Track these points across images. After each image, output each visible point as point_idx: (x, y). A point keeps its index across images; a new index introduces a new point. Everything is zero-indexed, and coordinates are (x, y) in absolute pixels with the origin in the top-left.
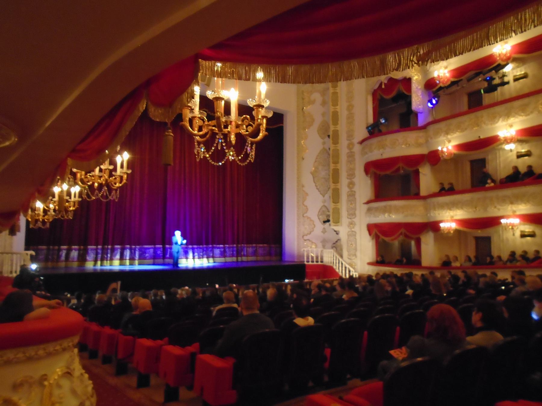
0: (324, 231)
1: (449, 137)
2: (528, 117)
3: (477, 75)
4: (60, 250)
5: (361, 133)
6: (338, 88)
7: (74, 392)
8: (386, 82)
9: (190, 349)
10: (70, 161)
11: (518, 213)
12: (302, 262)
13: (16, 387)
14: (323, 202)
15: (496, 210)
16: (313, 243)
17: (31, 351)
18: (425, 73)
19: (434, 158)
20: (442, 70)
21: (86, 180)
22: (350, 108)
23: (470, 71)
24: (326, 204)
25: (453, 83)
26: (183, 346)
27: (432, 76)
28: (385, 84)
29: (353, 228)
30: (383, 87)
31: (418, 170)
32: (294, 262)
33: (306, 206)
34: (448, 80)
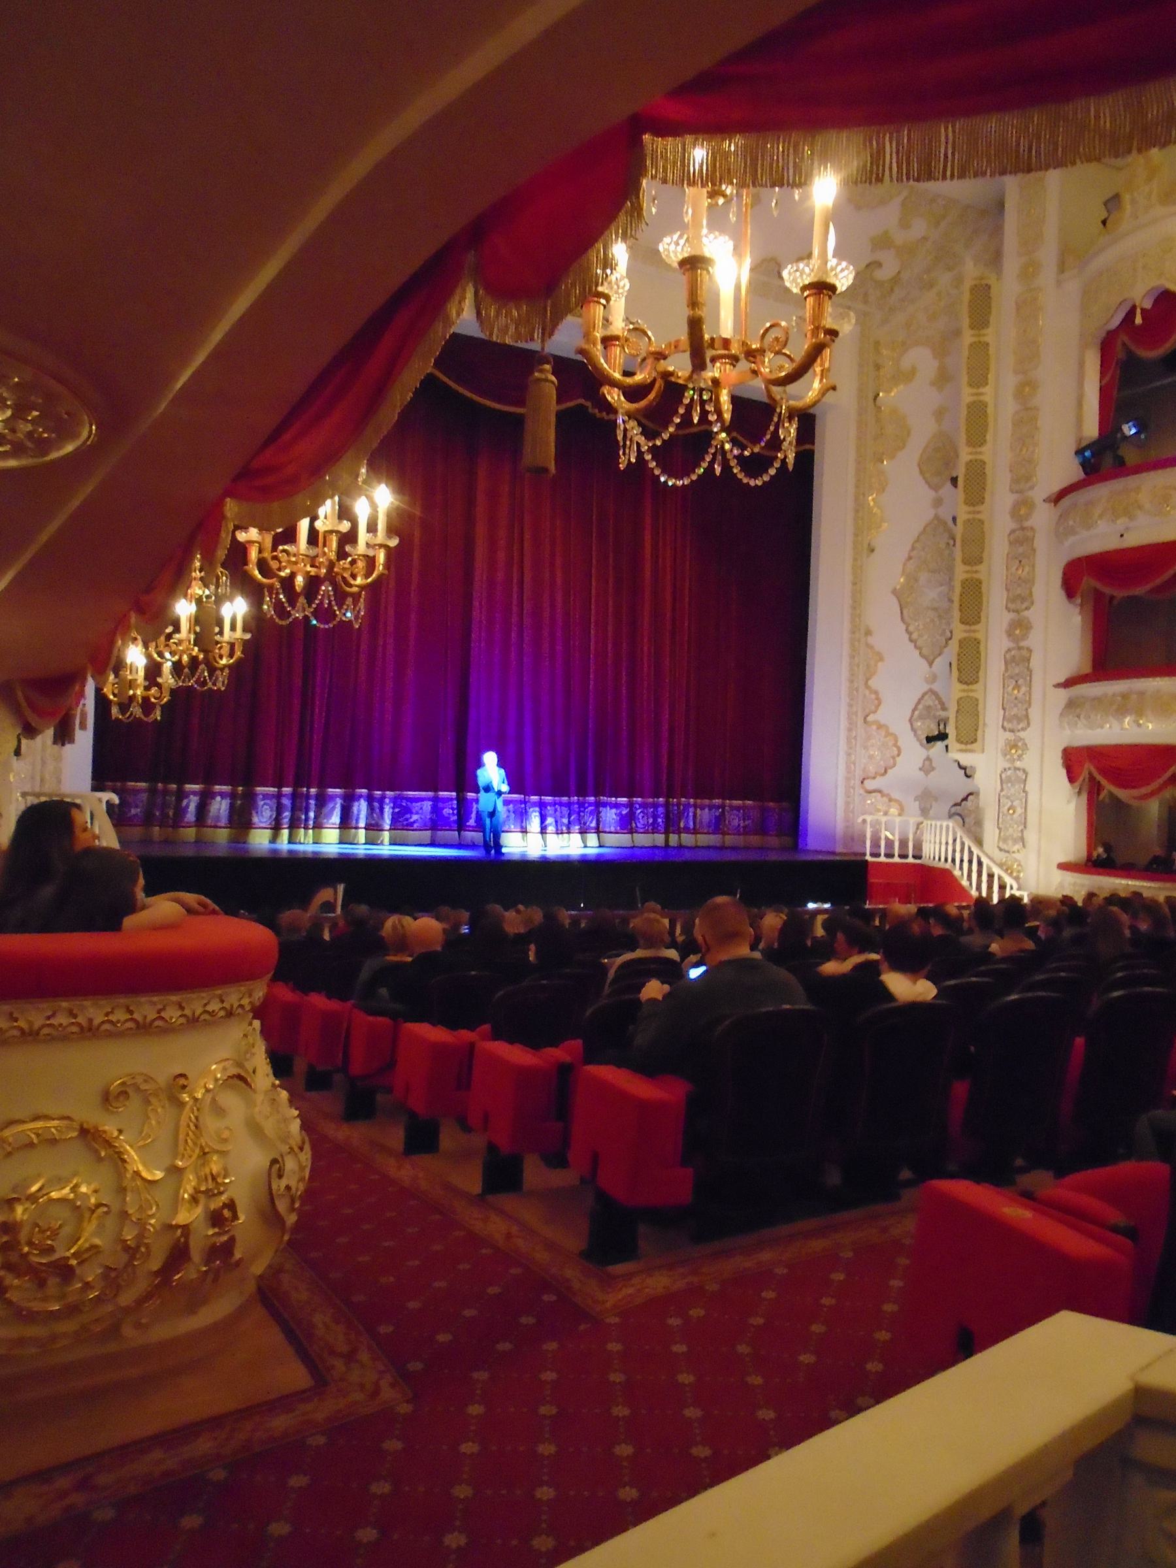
0: (928, 767)
4: (181, 795)
5: (1058, 465)
6: (989, 330)
7: (255, 1130)
8: (1148, 305)
9: (557, 1053)
10: (231, 507)
12: (855, 854)
13: (108, 1099)
14: (927, 681)
16: (890, 800)
17: (146, 1008)
21: (274, 565)
22: (1026, 390)
24: (936, 687)
26: (533, 1042)
29: (1020, 757)
30: (1138, 320)
32: (834, 853)
33: (876, 693)
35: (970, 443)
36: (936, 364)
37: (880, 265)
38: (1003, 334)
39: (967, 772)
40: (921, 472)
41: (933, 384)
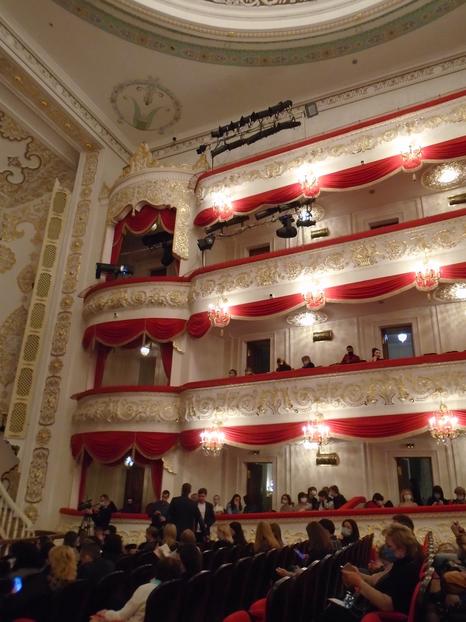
1: (225, 293)
2: (341, 271)
3: (271, 212)
5: (87, 278)
8: (138, 209)
11: (326, 417)
15: (292, 411)
18: (197, 200)
19: (198, 326)
20: (224, 198)
23: (263, 203)
25: (238, 220)
27: (208, 206)
28: (136, 211)
30: (133, 214)
31: (171, 343)
34: (231, 214)
35: (44, 265)
36: (35, 232)
37: (12, 174)
38: (69, 217)
39: (15, 449)
40: (18, 282)
41: (32, 240)
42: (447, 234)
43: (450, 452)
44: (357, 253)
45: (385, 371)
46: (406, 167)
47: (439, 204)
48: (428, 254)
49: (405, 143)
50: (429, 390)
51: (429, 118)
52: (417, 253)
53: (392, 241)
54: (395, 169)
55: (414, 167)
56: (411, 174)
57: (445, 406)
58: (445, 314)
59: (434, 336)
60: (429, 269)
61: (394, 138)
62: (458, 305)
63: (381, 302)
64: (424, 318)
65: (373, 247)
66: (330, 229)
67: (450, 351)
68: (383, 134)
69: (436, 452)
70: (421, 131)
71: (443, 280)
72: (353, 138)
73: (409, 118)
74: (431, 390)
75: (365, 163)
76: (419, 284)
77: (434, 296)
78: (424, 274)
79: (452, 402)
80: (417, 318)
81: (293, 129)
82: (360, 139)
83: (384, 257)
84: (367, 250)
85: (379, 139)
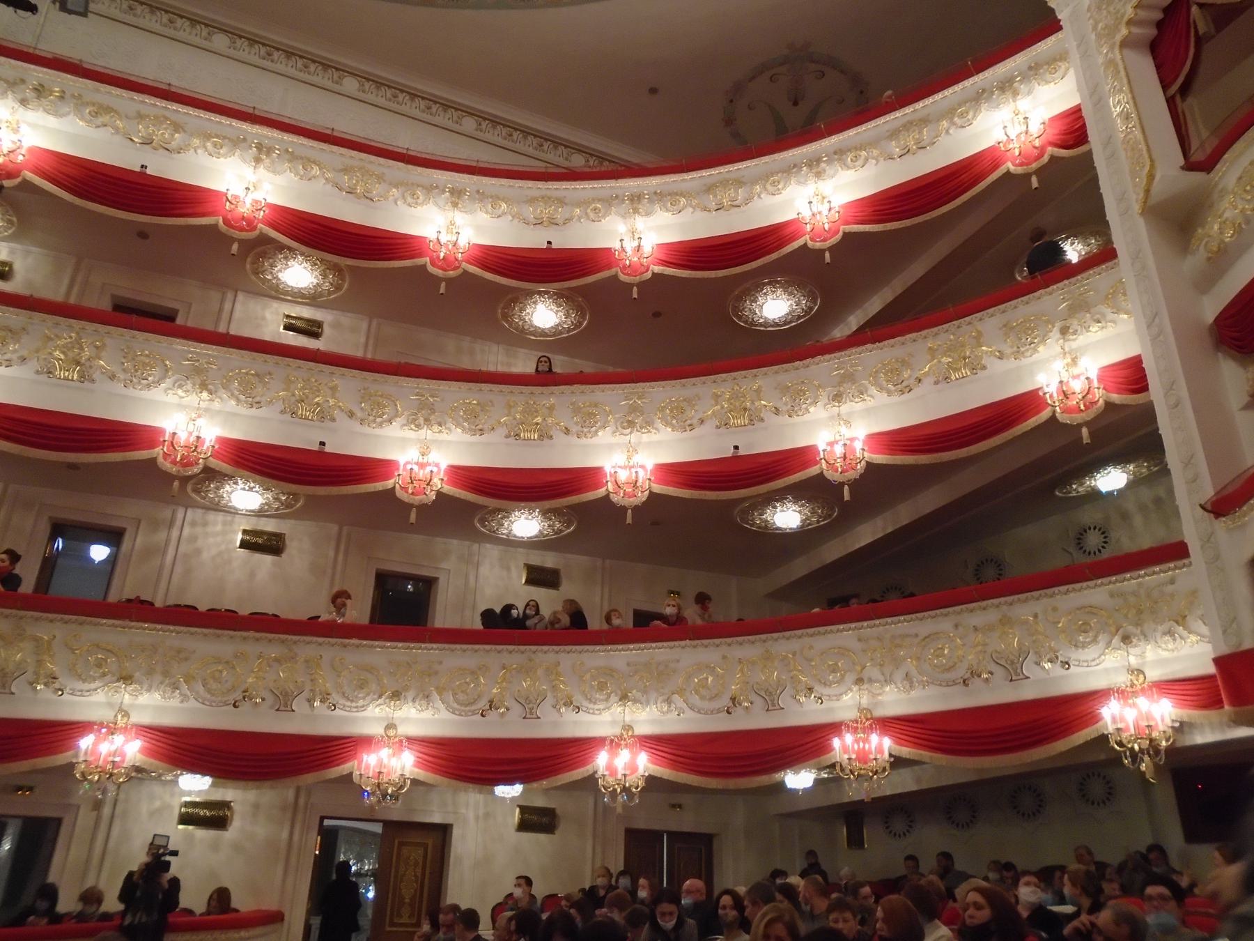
42: (254, 380)
43: (107, 811)
44: (56, 347)
45: (21, 618)
46: (226, 222)
47: (264, 318)
48: (203, 405)
49: (244, 180)
50: (104, 675)
51: (302, 158)
52: (183, 395)
53: (142, 351)
54: (203, 215)
55: (241, 229)
56: (233, 240)
57: (127, 715)
58: (199, 530)
59: (161, 567)
60: (195, 434)
61: (225, 156)
62: (229, 518)
63: (73, 466)
64: (155, 525)
65: (97, 347)
66: (18, 266)
67: (182, 603)
68: (208, 137)
69: (78, 807)
70: (279, 173)
71: (215, 463)
72: (145, 110)
73: (267, 137)
74: (108, 678)
75: (149, 171)
76: (166, 455)
77: (189, 488)
78: (183, 437)
79: (144, 707)
80: (140, 521)
81: (11, 9)
82: (159, 120)
83: (113, 377)
84: (81, 348)
85: (196, 142)
